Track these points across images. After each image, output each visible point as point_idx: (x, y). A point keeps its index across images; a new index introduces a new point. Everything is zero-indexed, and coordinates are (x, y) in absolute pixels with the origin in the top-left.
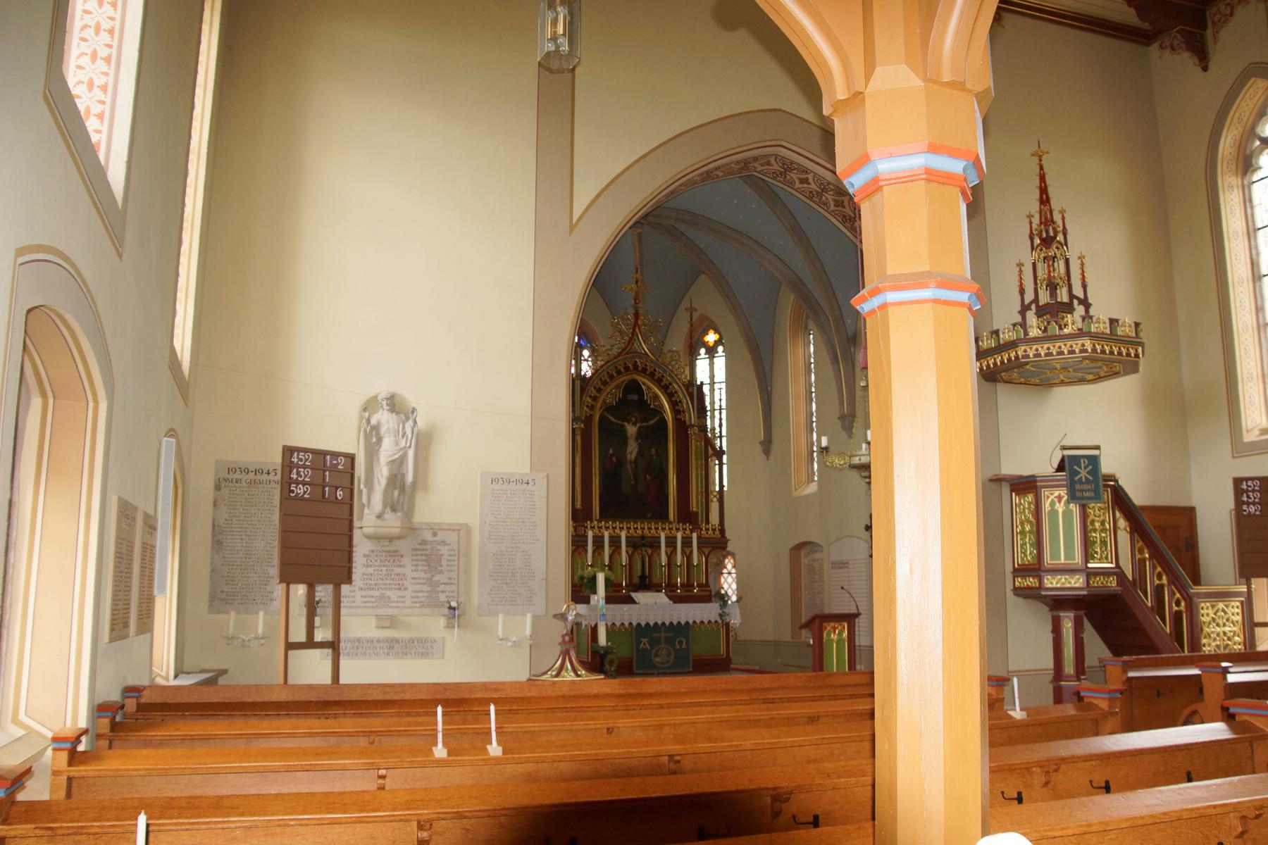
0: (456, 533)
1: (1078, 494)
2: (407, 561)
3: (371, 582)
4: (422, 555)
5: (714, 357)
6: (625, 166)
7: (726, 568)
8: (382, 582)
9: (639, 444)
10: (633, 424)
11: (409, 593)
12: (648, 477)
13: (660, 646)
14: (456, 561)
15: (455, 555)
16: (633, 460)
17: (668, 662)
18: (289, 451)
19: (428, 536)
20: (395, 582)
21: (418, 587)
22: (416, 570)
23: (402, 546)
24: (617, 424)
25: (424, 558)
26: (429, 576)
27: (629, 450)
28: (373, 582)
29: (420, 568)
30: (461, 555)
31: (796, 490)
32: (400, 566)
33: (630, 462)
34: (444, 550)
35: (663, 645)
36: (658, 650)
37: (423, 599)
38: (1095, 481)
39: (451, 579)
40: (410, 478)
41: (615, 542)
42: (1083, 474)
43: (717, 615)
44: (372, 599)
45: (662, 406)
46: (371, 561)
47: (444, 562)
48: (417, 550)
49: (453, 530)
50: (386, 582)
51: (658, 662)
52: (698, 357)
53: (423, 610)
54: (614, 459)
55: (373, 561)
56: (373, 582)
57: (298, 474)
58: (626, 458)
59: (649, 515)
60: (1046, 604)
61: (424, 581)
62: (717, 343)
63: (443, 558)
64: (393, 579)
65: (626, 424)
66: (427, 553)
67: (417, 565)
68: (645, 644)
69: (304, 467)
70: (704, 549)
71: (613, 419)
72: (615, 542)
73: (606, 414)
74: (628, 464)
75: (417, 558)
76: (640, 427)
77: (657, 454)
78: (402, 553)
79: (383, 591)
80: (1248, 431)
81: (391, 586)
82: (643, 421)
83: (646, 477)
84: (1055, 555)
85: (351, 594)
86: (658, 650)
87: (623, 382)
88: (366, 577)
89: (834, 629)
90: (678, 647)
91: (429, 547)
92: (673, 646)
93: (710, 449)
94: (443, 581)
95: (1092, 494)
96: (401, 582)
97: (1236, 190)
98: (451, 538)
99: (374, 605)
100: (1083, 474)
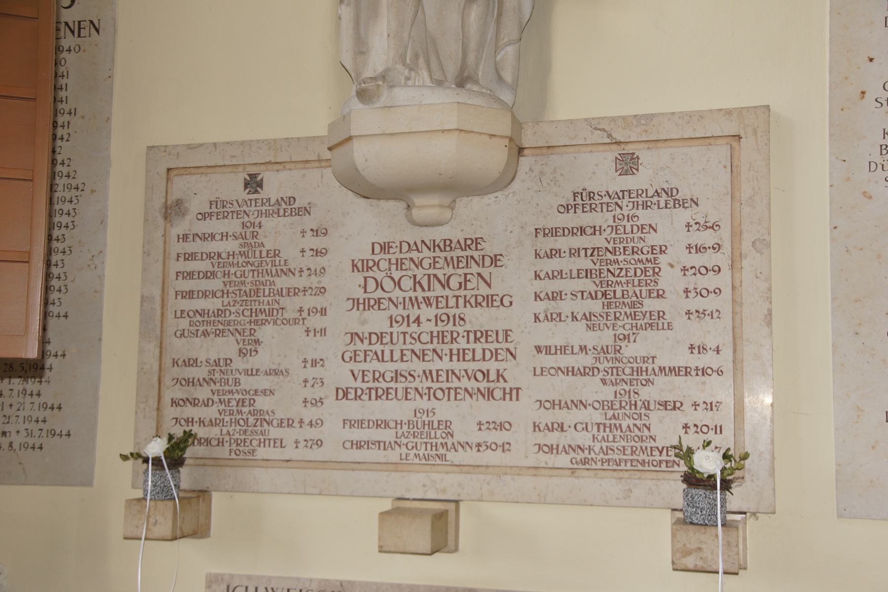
0: (721, 152)
3: (380, 367)
4: (574, 253)
8: (418, 366)
14: (726, 272)
15: (716, 248)
20: (472, 366)
22: (555, 317)
25: (585, 263)
26: (606, 337)
28: (388, 368)
29: (566, 307)
30: (746, 245)
32: (489, 300)
37: (583, 438)
39: (702, 349)
44: (387, 435)
46: (379, 285)
48: (554, 232)
49: (707, 140)
50: (436, 365)
55: (388, 284)
56: (388, 368)
61: (586, 360)
63: (663, 259)
64: (461, 355)
66: (599, 241)
67: (556, 296)
75: (554, 264)
78: (489, 248)
79: (423, 404)
81: (455, 383)
85: (310, 414)
88: (360, 346)
91: (602, 219)
94: (659, 362)
96: (492, 366)
99: (393, 456)
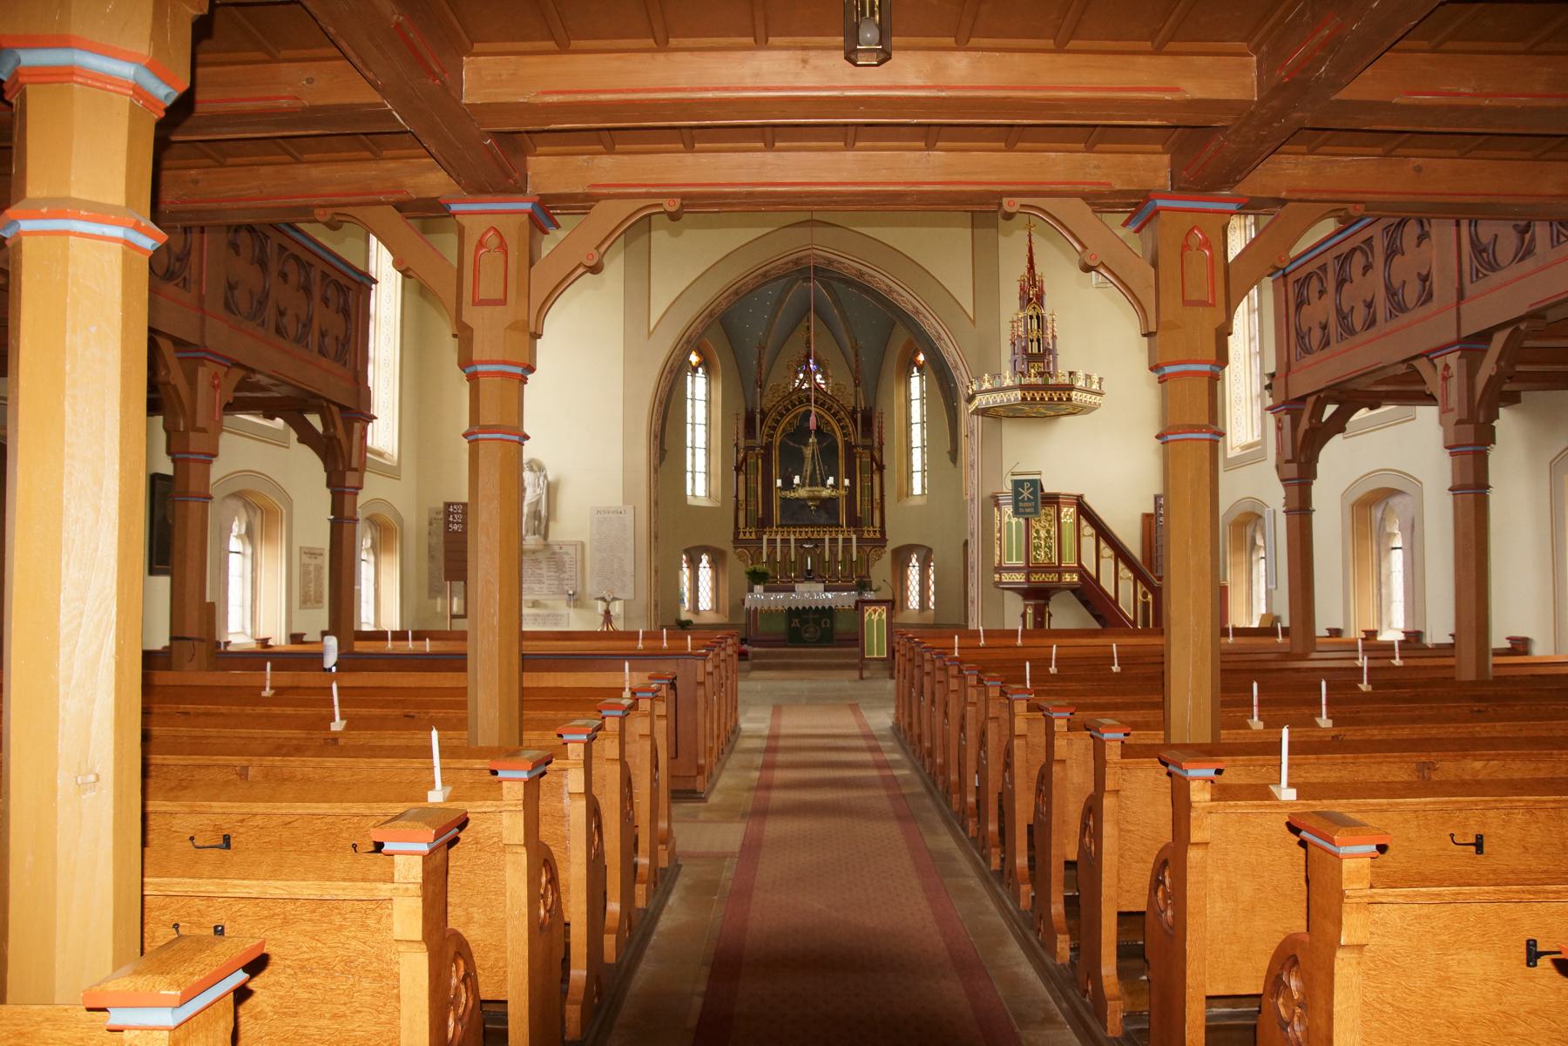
1: (1021, 510)
2: (544, 565)
6: (688, 284)
11: (545, 586)
18: (448, 505)
19: (556, 548)
21: (552, 582)
23: (540, 556)
34: (567, 558)
38: (1036, 497)
40: (543, 513)
41: (785, 541)
42: (1026, 494)
45: (833, 430)
47: (567, 566)
53: (556, 597)
57: (454, 518)
60: (1019, 594)
69: (458, 513)
71: (791, 444)
72: (785, 541)
80: (1232, 449)
84: (1010, 558)
89: (875, 611)
92: (820, 624)
95: (1032, 510)
97: (1238, 232)
98: (571, 550)
100: (1026, 494)
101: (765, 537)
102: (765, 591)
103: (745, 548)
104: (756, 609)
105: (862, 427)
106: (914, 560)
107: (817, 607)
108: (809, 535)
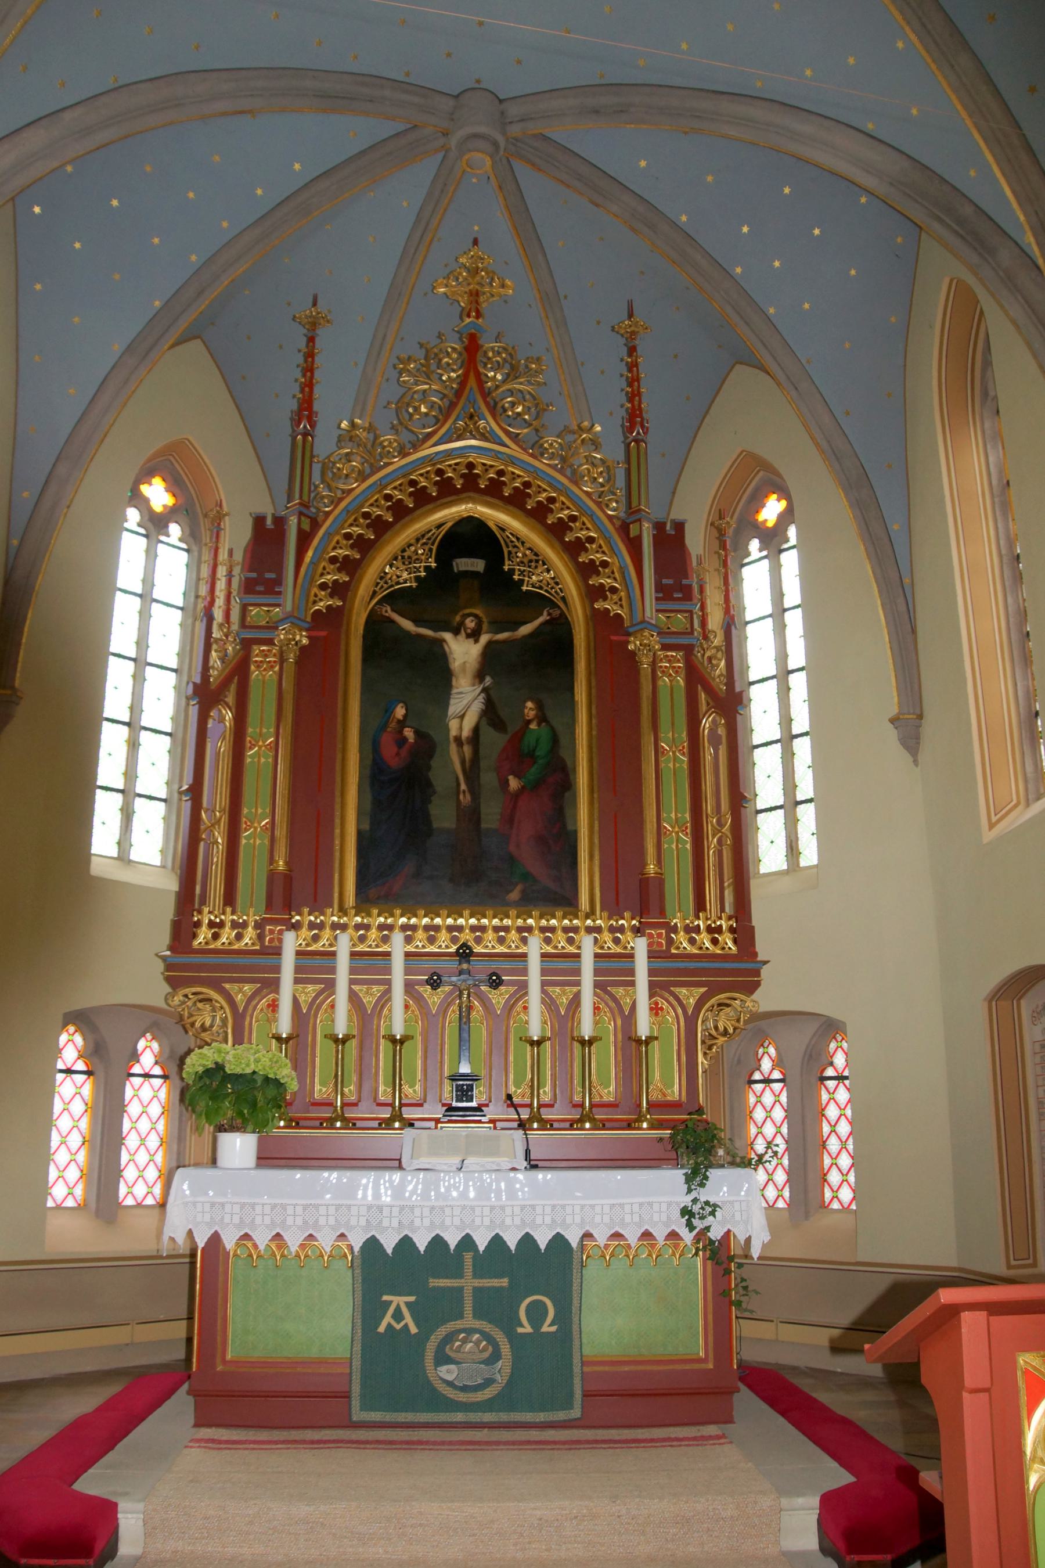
5: (781, 551)
7: (831, 1064)
9: (485, 690)
10: (468, 636)
12: (514, 783)
13: (459, 1324)
16: (466, 733)
17: (489, 1382)
24: (419, 636)
27: (455, 706)
31: (991, 826)
33: (458, 740)
35: (469, 1321)
36: (449, 1338)
43: (677, 1213)
51: (450, 1384)
52: (746, 560)
54: (409, 733)
58: (447, 730)
59: (515, 895)
62: (786, 518)
65: (447, 636)
68: (398, 1316)
70: (683, 991)
71: (407, 625)
73: (388, 611)
74: (453, 748)
76: (490, 644)
77: (542, 719)
82: (498, 626)
83: (506, 783)
86: (449, 1338)
87: (439, 526)
90: (527, 1329)
92: (509, 1323)
93: (703, 696)
101: (291, 943)
102: (266, 1159)
103: (216, 984)
104: (215, 1239)
105: (660, 571)
106: (766, 1064)
107: (497, 1241)
108: (467, 936)
